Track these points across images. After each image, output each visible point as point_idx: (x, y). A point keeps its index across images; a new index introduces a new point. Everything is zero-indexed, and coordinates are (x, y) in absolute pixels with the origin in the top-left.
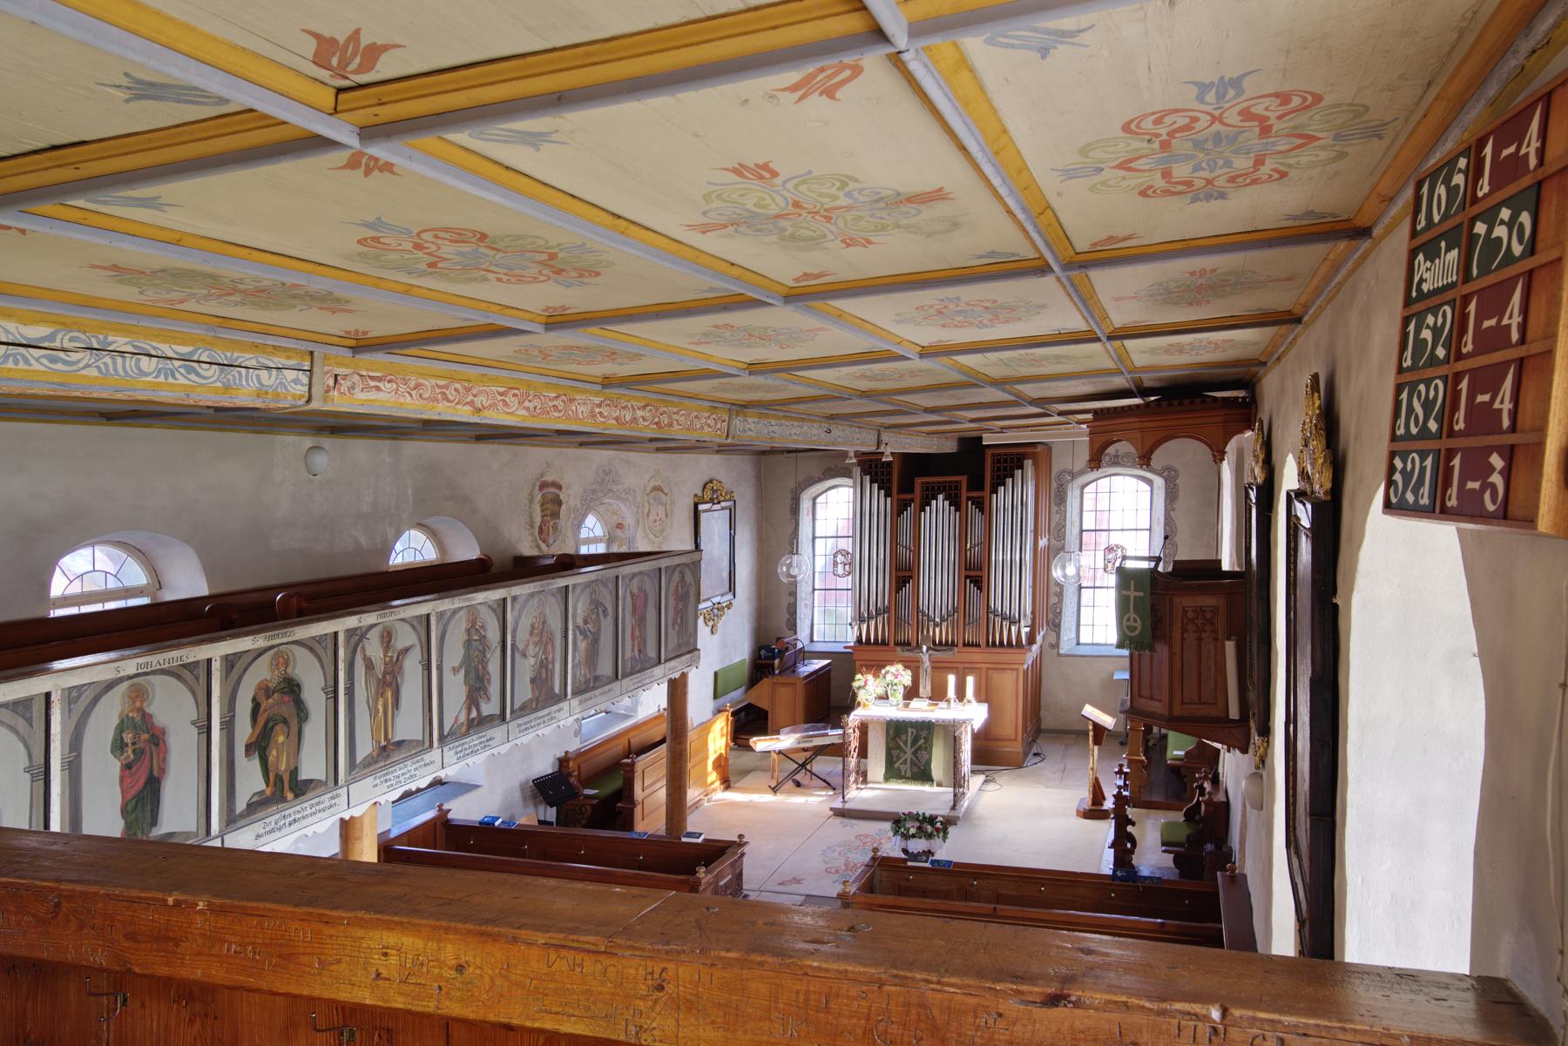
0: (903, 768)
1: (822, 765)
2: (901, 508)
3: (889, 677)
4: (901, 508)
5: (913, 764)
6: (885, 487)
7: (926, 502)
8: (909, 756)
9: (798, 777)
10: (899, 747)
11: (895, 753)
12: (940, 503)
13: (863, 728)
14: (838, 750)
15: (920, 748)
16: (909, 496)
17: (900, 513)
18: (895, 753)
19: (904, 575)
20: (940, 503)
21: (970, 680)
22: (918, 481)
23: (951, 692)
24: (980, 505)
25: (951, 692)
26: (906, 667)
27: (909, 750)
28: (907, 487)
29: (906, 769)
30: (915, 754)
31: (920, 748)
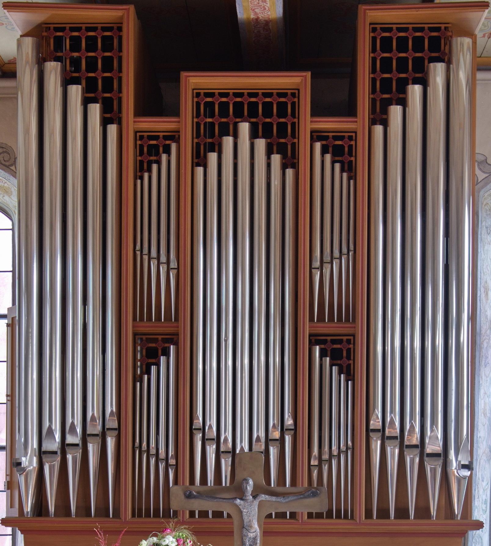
7: (207, 143)
12: (243, 145)
17: (142, 168)
19: (154, 340)
20: (243, 145)
22: (195, 81)
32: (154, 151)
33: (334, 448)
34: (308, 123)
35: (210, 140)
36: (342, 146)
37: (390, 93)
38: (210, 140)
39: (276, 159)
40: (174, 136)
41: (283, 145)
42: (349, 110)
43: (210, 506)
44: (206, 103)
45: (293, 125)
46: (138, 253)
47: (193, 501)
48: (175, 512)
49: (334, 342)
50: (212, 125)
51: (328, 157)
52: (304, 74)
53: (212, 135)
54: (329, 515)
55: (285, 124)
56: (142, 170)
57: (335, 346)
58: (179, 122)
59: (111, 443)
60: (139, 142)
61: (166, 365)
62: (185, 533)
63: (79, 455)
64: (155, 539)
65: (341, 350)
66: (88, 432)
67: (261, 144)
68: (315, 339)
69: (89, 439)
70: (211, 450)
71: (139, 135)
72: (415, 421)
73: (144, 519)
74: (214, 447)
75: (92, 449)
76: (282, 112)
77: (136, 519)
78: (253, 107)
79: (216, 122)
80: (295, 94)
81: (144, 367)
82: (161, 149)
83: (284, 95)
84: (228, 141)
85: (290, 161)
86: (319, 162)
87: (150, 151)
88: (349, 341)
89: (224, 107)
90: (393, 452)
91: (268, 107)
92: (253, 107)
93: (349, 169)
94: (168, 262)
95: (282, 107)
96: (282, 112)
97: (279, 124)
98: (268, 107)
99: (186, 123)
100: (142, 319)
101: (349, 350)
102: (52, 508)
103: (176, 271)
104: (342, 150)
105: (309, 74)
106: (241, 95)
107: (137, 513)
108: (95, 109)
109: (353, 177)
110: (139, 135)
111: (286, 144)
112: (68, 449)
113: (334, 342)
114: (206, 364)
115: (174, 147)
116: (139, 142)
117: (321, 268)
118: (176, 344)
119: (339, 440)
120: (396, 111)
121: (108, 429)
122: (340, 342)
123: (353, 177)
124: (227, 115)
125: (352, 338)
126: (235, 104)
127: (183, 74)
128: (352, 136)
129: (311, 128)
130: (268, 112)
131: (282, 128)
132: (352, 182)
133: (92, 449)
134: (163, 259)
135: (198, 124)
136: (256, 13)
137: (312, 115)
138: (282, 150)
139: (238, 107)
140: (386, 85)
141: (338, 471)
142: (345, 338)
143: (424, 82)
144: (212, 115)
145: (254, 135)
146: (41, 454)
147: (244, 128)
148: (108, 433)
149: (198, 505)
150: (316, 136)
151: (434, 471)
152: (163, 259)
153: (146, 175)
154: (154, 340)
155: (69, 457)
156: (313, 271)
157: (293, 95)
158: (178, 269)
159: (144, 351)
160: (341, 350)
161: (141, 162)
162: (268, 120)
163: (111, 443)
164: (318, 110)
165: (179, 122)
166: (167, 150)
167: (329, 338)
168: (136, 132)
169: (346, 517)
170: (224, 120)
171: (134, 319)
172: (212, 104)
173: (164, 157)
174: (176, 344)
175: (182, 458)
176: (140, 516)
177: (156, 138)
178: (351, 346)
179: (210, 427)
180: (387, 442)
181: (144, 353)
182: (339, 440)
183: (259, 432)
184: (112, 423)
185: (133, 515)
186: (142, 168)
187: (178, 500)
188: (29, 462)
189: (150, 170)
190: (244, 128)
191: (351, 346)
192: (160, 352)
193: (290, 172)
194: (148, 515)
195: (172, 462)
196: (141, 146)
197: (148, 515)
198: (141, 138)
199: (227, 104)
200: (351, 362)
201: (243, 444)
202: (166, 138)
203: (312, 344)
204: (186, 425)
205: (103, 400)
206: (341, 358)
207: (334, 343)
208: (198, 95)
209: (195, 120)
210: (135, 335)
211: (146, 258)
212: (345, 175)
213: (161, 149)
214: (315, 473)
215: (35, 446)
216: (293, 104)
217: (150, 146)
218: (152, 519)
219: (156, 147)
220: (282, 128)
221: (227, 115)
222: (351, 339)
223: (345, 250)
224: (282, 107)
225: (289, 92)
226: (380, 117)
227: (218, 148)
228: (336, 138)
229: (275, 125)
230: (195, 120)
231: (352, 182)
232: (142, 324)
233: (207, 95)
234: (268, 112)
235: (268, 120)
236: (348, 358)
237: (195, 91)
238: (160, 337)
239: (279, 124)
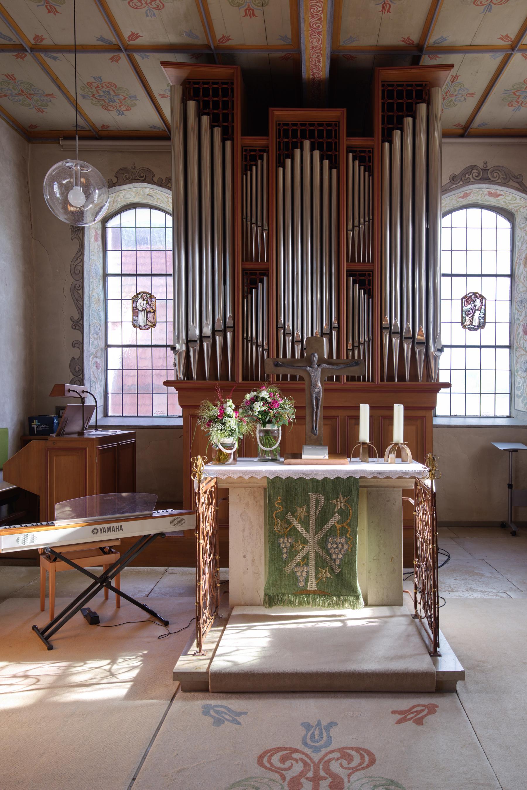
0: (301, 572)
1: (137, 582)
3: (258, 407)
5: (321, 563)
6: (221, 121)
8: (312, 548)
9: (93, 605)
10: (292, 532)
11: (285, 543)
12: (307, 158)
13: (221, 496)
14: (176, 551)
15: (332, 532)
16: (257, 141)
17: (246, 169)
18: (285, 543)
19: (253, 275)
20: (307, 158)
21: (399, 411)
23: (364, 434)
24: (367, 160)
25: (364, 434)
26: (285, 392)
27: (313, 538)
29: (309, 576)
30: (323, 543)
31: (332, 532)
32: (254, 159)
33: (361, 339)
34: (345, 141)
35: (287, 152)
36: (365, 157)
38: (287, 152)
39: (326, 163)
40: (265, 149)
41: (330, 154)
43: (289, 372)
45: (336, 143)
46: (245, 220)
47: (279, 368)
48: (268, 376)
49: (360, 275)
50: (288, 143)
51: (357, 162)
52: (343, 109)
53: (288, 149)
54: (359, 379)
55: (331, 143)
56: (246, 170)
57: (361, 278)
58: (268, 139)
59: (229, 335)
60: (244, 153)
61: (262, 289)
62: (274, 389)
63: (210, 343)
64: (255, 393)
65: (365, 280)
66: (215, 329)
67: (317, 154)
68: (350, 273)
69: (216, 333)
70: (289, 340)
71: (245, 149)
72: (409, 323)
73: (249, 382)
74: (291, 338)
75: (219, 340)
76: (329, 136)
77: (245, 382)
78: (312, 132)
79: (289, 141)
80: (337, 125)
81: (249, 290)
82: (258, 157)
83: (330, 125)
84: (297, 152)
86: (352, 164)
87: (250, 159)
88: (369, 275)
89: (295, 132)
90: (396, 342)
91: (320, 132)
92: (312, 132)
93: (370, 170)
94: (262, 226)
95: (329, 132)
96: (329, 136)
97: (327, 143)
98: (320, 132)
99: (272, 140)
100: (247, 260)
101: (369, 280)
102: (194, 376)
103: (267, 231)
105: (345, 110)
106: (304, 125)
107: (245, 377)
108: (218, 132)
109: (371, 174)
110: (245, 149)
111: (331, 155)
112: (204, 339)
113: (360, 275)
115: (265, 155)
116: (244, 153)
117: (353, 230)
118: (268, 276)
119: (365, 334)
121: (228, 327)
122: (364, 275)
124: (296, 137)
125: (371, 273)
126: (301, 130)
127: (271, 109)
128: (370, 150)
129: (347, 144)
130: (321, 136)
131: (329, 145)
132: (371, 178)
133: (219, 340)
134: (259, 224)
135: (279, 142)
136: (313, 74)
137: (347, 136)
138: (329, 158)
139: (303, 132)
141: (364, 352)
142: (367, 273)
144: (288, 138)
145: (312, 149)
147: (307, 144)
148: (228, 329)
149: (282, 371)
150: (350, 149)
151: (420, 353)
152: (259, 224)
153: (249, 173)
154: (253, 275)
155: (205, 344)
156: (348, 232)
157: (336, 125)
158: (268, 230)
159: (249, 280)
160: (365, 280)
161: (246, 165)
162: (321, 140)
163: (229, 335)
164: (351, 134)
165: (268, 139)
166: (261, 158)
167: (357, 273)
168: (242, 147)
169: (369, 380)
170: (295, 140)
171: (243, 260)
172: (287, 130)
173: (259, 162)
174: (268, 276)
176: (247, 380)
177: (255, 151)
178: (371, 278)
179: (288, 326)
180: (393, 335)
181: (249, 282)
182: (365, 334)
183: (317, 330)
184: (230, 323)
185: (243, 380)
187: (269, 368)
189: (251, 171)
190: (307, 144)
191: (371, 278)
192: (258, 281)
193: (334, 171)
194: (252, 379)
195: (266, 347)
196: (246, 156)
197: (252, 379)
198: (246, 150)
199: (297, 130)
200: (371, 287)
202: (260, 151)
203: (348, 276)
204: (275, 326)
205: (224, 311)
206: (365, 285)
208: (279, 124)
209: (278, 140)
210: (243, 270)
211: (249, 223)
212: (367, 173)
213: (258, 157)
214: (350, 354)
215: (184, 337)
216: (336, 130)
217: (251, 156)
218: (254, 382)
219: (255, 156)
220: (329, 145)
221: (296, 137)
223: (367, 219)
224: (329, 132)
225: (333, 123)
226: (388, 138)
227: (292, 157)
228: (361, 152)
230: (278, 140)
231: (371, 178)
232: (247, 263)
233: (285, 125)
234: (321, 136)
235: (321, 140)
236: (369, 285)
237: (277, 122)
238: (258, 272)
239: (327, 143)
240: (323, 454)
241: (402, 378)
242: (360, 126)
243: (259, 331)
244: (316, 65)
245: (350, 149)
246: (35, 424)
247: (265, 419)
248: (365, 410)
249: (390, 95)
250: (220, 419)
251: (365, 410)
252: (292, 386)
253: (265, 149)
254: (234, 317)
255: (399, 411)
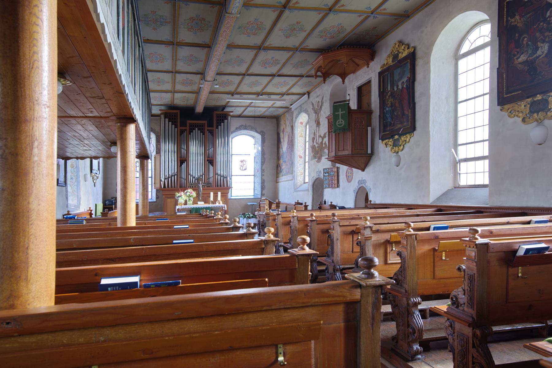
2: (182, 132)
4: (182, 132)
7: (191, 131)
17: (181, 135)
19: (183, 160)
21: (219, 194)
28: (183, 124)
34: (206, 128)
37: (219, 124)
40: (186, 130)
42: (212, 126)
44: (191, 125)
61: (184, 165)
67: (199, 131)
68: (208, 160)
71: (180, 130)
80: (204, 124)
85: (204, 134)
90: (219, 177)
93: (213, 135)
99: (188, 128)
104: (212, 133)
114: (191, 163)
120: (220, 127)
123: (213, 135)
140: (218, 123)
141: (211, 180)
143: (224, 122)
146: (165, 179)
147: (197, 129)
150: (208, 130)
154: (183, 160)
175: (187, 179)
186: (181, 135)
188: (163, 180)
190: (197, 129)
201: (196, 176)
204: (188, 173)
207: (210, 161)
222: (213, 160)
226: (217, 128)
229: (202, 129)
240: (203, 203)
241: (221, 186)
242: (210, 124)
243: (184, 175)
244: (199, 109)
245: (208, 130)
246: (107, 202)
247: (189, 196)
248: (212, 194)
249: (218, 117)
250: (181, 196)
251: (212, 194)
252: (195, 188)
253: (186, 130)
254: (177, 172)
255: (219, 194)
